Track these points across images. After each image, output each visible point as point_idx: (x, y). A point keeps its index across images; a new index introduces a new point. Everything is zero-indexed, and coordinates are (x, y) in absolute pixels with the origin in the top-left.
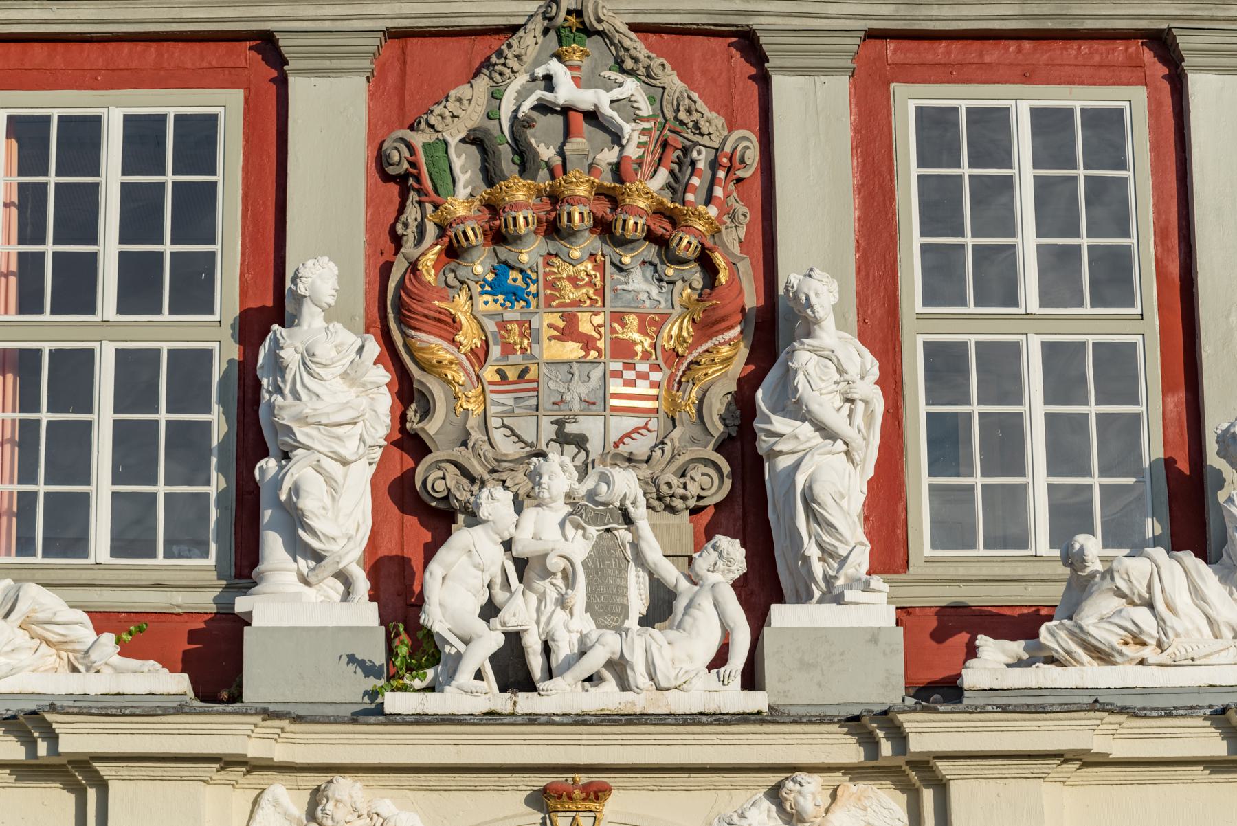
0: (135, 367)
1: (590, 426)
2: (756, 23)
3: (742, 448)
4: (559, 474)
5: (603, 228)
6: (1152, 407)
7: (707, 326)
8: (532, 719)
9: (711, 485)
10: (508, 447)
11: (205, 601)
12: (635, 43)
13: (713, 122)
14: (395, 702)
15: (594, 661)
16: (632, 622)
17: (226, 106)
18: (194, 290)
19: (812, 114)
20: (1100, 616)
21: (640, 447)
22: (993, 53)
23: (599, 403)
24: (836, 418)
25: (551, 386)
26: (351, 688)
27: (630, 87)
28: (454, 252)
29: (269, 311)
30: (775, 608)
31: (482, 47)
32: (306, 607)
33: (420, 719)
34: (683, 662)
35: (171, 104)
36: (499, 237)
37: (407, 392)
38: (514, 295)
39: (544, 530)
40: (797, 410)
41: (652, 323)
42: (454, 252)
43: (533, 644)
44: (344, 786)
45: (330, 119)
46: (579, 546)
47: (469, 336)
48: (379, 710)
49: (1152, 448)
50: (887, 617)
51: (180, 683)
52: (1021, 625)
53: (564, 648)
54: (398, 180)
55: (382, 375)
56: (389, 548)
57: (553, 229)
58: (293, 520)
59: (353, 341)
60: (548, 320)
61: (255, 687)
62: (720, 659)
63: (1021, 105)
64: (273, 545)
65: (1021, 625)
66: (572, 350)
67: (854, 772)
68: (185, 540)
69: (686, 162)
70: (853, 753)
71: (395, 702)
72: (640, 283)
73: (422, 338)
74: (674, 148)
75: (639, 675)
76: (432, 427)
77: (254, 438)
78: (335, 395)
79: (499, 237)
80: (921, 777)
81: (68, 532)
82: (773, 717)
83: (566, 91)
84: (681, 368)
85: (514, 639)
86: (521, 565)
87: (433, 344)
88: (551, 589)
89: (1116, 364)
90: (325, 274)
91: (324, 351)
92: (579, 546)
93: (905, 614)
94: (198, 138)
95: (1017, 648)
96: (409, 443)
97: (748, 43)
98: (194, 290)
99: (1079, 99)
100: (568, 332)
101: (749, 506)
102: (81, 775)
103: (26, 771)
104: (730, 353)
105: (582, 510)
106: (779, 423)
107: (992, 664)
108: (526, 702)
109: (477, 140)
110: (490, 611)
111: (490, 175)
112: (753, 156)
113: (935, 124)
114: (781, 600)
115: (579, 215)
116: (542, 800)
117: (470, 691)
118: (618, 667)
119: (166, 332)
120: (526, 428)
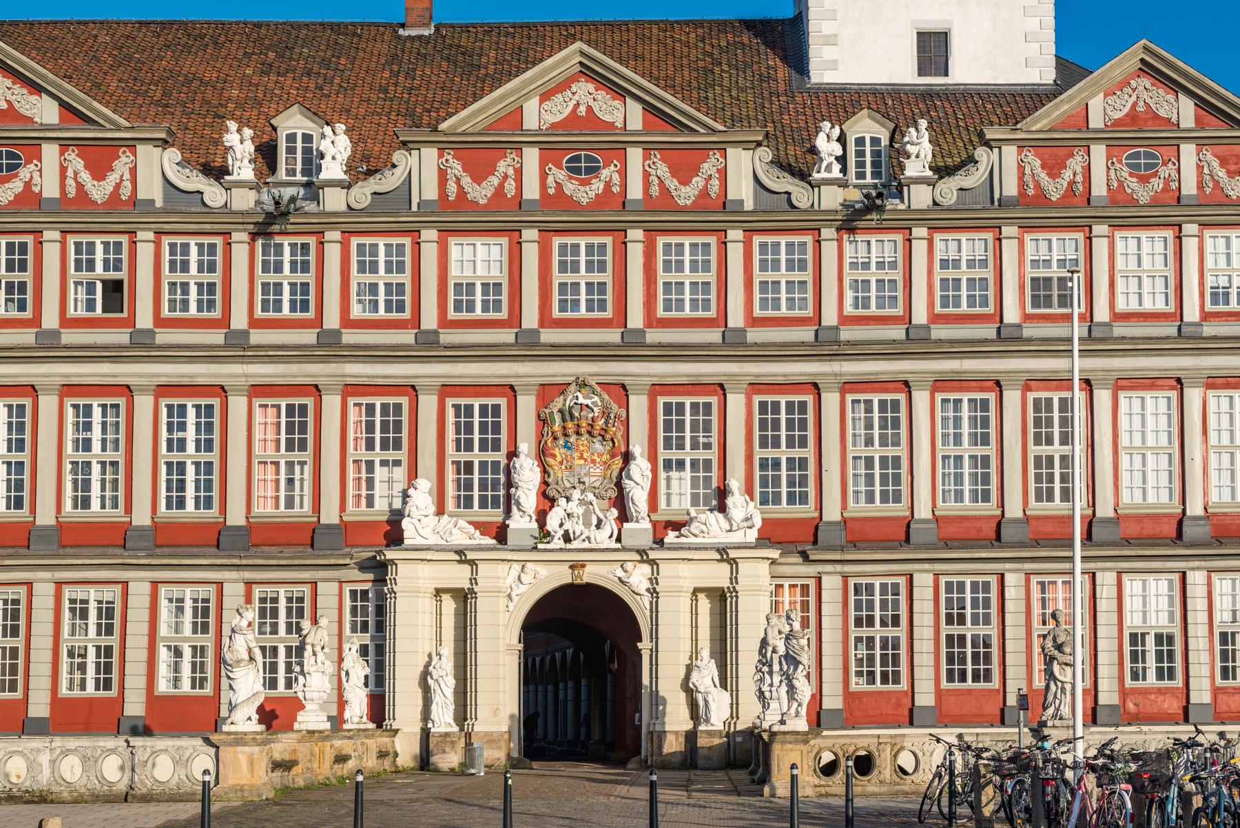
0: (483, 465)
1: (586, 479)
2: (626, 383)
3: (619, 485)
4: (576, 494)
5: (589, 433)
6: (715, 474)
7: (613, 456)
8: (569, 550)
9: (613, 494)
10: (568, 485)
11: (500, 519)
12: (598, 388)
13: (615, 407)
14: (540, 546)
15: (583, 537)
16: (593, 528)
17: (503, 402)
18: (496, 448)
19: (639, 404)
20: (694, 528)
21: (597, 484)
22: (681, 389)
23: (588, 474)
24: (639, 481)
25: (577, 470)
26: (531, 542)
27: (596, 398)
28: (555, 439)
29: (513, 454)
30: (625, 525)
31: (562, 388)
32: (522, 523)
33: (545, 550)
34: (603, 538)
35: (490, 401)
36: (566, 435)
37: (545, 471)
38: (569, 448)
39: (574, 507)
40: (630, 478)
41: (600, 455)
42: (555, 439)
43: (571, 532)
44: (529, 565)
45: (527, 405)
46: (580, 511)
47: (559, 459)
48: (535, 548)
49: (715, 484)
50: (649, 526)
51: (494, 542)
52: (677, 526)
53: (577, 533)
54: (543, 421)
55: (538, 470)
56: (541, 507)
57: (578, 433)
58: (518, 504)
59: (530, 461)
60: (576, 455)
61: (512, 540)
62: (611, 537)
63: (688, 401)
64: (514, 508)
65: (677, 526)
66: (582, 462)
67: (640, 562)
68: (495, 504)
69: (609, 416)
70: (639, 558)
71: (540, 546)
72: (598, 446)
73: (548, 459)
74: (606, 414)
75: (593, 540)
76: (550, 480)
77: (510, 484)
78: (528, 474)
79: (566, 435)
80: (653, 563)
81: (468, 503)
82: (624, 549)
83: (581, 400)
84: (609, 467)
85: (567, 532)
86: (568, 515)
87: (550, 460)
88: (575, 520)
89: (708, 464)
90: (524, 447)
91: (525, 465)
92: (580, 511)
93: (655, 524)
94: (496, 408)
95: (677, 533)
96: (545, 483)
97: (624, 387)
98: (496, 448)
99: (701, 400)
100: (581, 457)
101: (621, 502)
102: (472, 563)
103: (460, 562)
104: (618, 462)
105: (582, 502)
106: (627, 481)
107: (671, 537)
108: (568, 546)
109: (560, 411)
110: (561, 525)
111: (564, 420)
112: (624, 415)
113: (668, 406)
114: (627, 521)
115: (583, 430)
116: (571, 567)
117: (558, 543)
118: (588, 538)
119: (490, 456)
120: (572, 480)
